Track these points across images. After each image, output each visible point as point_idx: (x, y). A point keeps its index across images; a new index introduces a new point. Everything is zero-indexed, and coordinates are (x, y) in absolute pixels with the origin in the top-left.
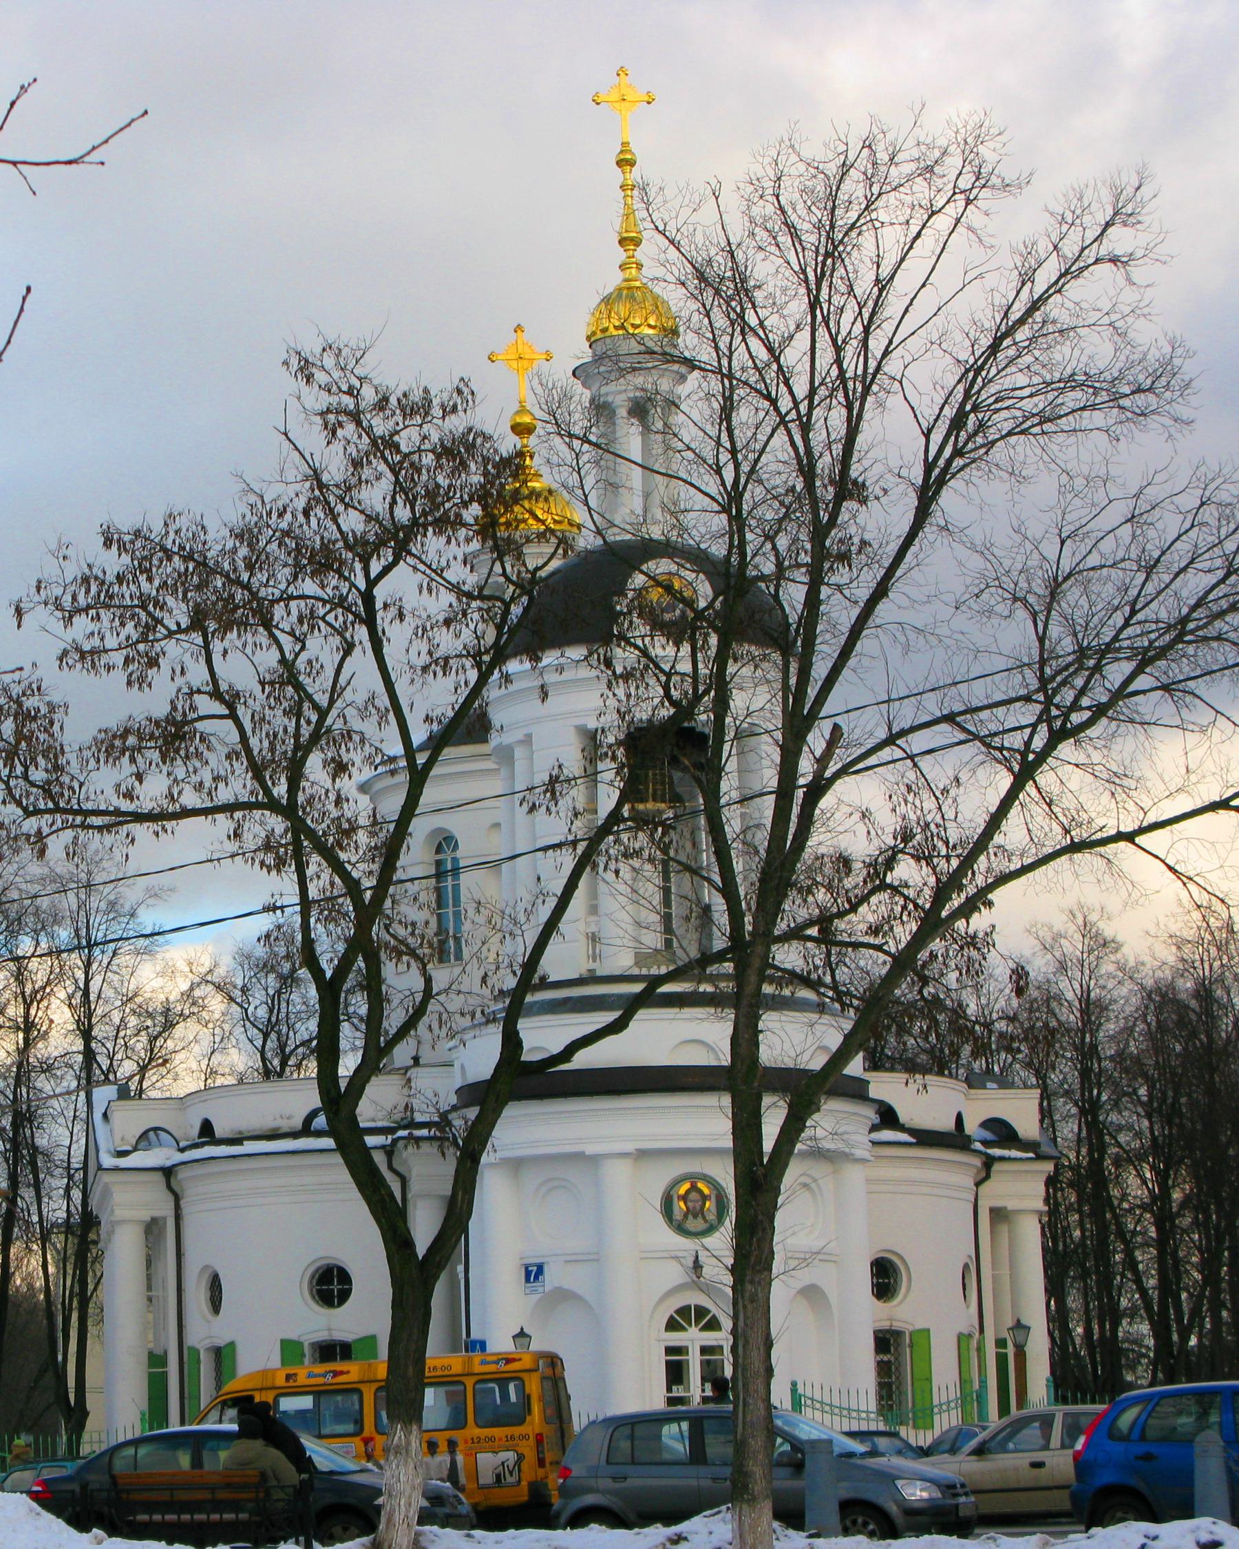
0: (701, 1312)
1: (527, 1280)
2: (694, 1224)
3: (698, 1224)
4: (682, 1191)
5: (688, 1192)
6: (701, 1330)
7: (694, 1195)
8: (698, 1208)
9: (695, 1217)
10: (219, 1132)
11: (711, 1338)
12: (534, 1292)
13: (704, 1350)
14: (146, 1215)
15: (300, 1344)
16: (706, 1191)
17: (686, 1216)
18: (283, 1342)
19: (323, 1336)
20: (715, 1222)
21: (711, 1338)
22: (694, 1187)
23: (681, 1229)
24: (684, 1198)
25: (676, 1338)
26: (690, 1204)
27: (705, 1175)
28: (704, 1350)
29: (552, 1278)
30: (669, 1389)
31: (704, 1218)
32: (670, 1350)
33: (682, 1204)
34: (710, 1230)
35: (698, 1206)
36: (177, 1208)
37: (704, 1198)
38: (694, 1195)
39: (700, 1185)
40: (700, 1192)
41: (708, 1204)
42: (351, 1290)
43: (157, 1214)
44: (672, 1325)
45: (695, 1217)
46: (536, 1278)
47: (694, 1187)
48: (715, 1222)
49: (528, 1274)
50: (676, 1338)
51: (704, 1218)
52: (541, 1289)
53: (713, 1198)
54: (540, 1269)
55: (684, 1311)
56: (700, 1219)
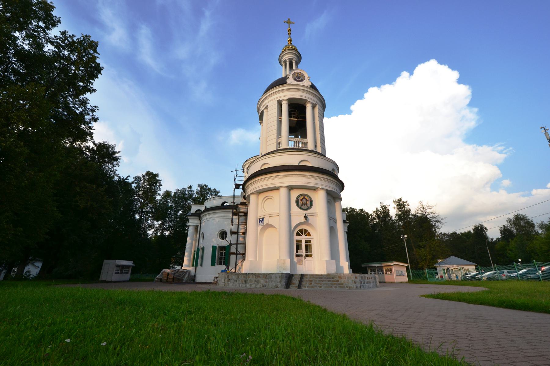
0: (306, 231)
1: (260, 223)
2: (303, 207)
3: (305, 207)
4: (301, 199)
5: (303, 199)
6: (306, 235)
7: (304, 200)
8: (305, 203)
9: (305, 205)
10: (207, 207)
11: (308, 238)
12: (261, 225)
13: (306, 241)
14: (195, 224)
15: (216, 247)
16: (307, 199)
17: (302, 205)
18: (213, 246)
19: (220, 245)
20: (310, 207)
21: (308, 238)
22: (304, 198)
23: (301, 208)
24: (302, 200)
25: (299, 238)
26: (303, 202)
27: (307, 195)
28: (306, 241)
29: (265, 222)
30: (297, 252)
31: (307, 205)
32: (297, 241)
33: (301, 201)
34: (308, 209)
35: (305, 202)
36: (201, 223)
37: (307, 201)
38: (304, 200)
39: (306, 197)
40: (306, 199)
41: (308, 202)
42: (227, 237)
43: (198, 224)
44: (298, 234)
45: (305, 205)
46: (262, 222)
47: (304, 198)
48: (310, 207)
49: (260, 221)
50: (299, 238)
51: (307, 205)
52: (263, 225)
53: (309, 201)
54: (263, 219)
55: (301, 231)
56: (306, 205)
